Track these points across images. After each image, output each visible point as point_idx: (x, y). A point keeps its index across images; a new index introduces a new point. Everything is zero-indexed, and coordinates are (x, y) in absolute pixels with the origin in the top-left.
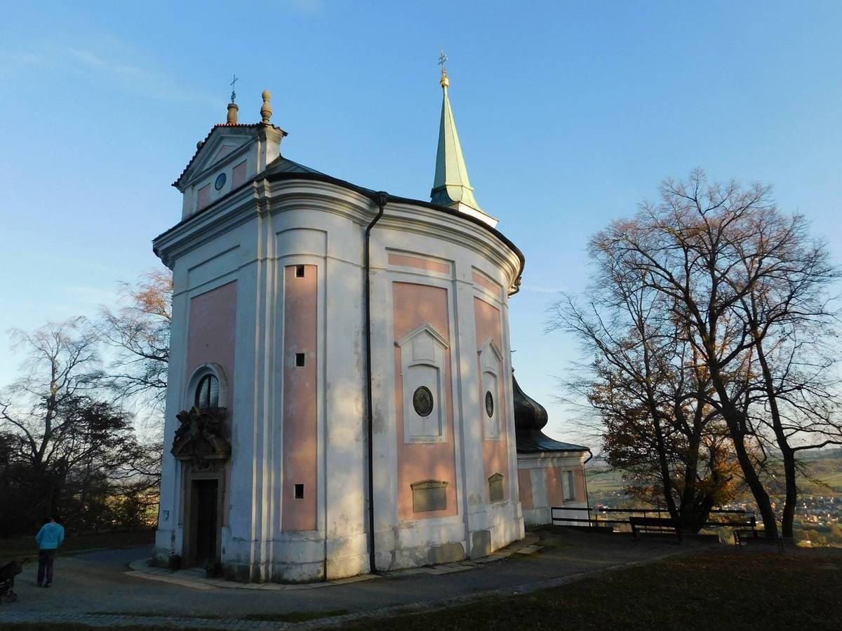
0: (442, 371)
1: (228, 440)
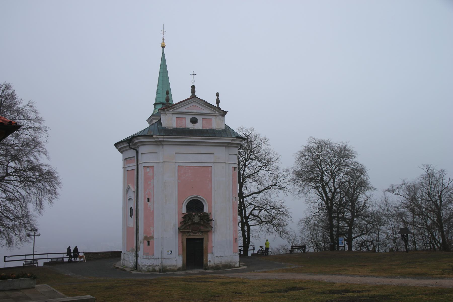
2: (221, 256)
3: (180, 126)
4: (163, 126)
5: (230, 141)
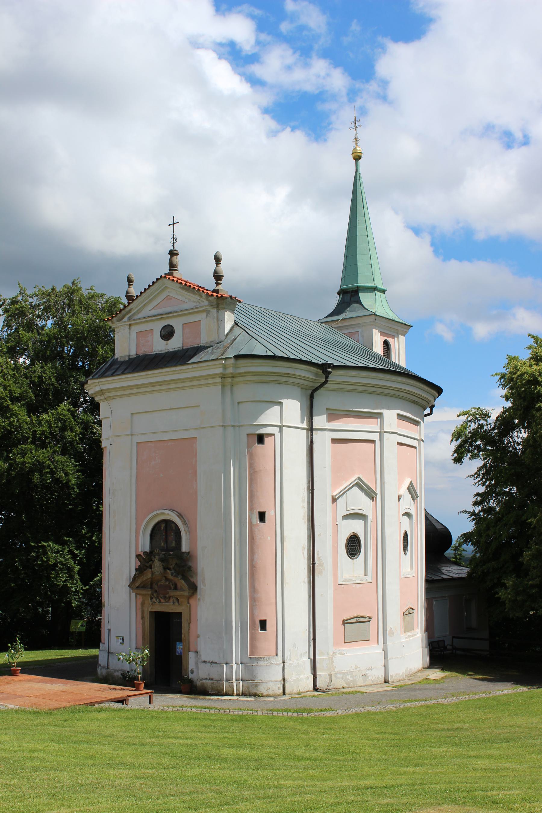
0: (370, 518)
1: (192, 580)
2: (212, 662)
3: (141, 352)
4: (116, 357)
5: (220, 370)
